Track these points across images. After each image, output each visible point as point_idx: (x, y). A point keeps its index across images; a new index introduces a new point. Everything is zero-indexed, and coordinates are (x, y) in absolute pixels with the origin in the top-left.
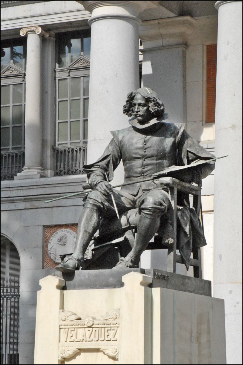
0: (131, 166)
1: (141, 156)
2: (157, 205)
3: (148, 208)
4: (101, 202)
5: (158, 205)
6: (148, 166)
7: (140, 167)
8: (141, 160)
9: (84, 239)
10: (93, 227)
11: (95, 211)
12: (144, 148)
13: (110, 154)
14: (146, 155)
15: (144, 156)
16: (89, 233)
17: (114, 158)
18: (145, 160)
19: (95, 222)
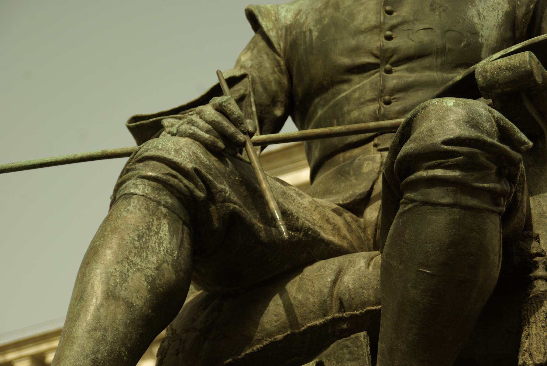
0: (336, 104)
1: (376, 56)
2: (482, 131)
3: (434, 145)
4: (196, 170)
5: (489, 134)
6: (409, 93)
7: (373, 100)
8: (378, 74)
9: (99, 334)
10: (152, 282)
11: (164, 210)
12: (387, 26)
13: (244, 76)
14: (394, 51)
15: (388, 54)
16: (130, 305)
17: (260, 89)
18: (389, 72)
19: (165, 261)
